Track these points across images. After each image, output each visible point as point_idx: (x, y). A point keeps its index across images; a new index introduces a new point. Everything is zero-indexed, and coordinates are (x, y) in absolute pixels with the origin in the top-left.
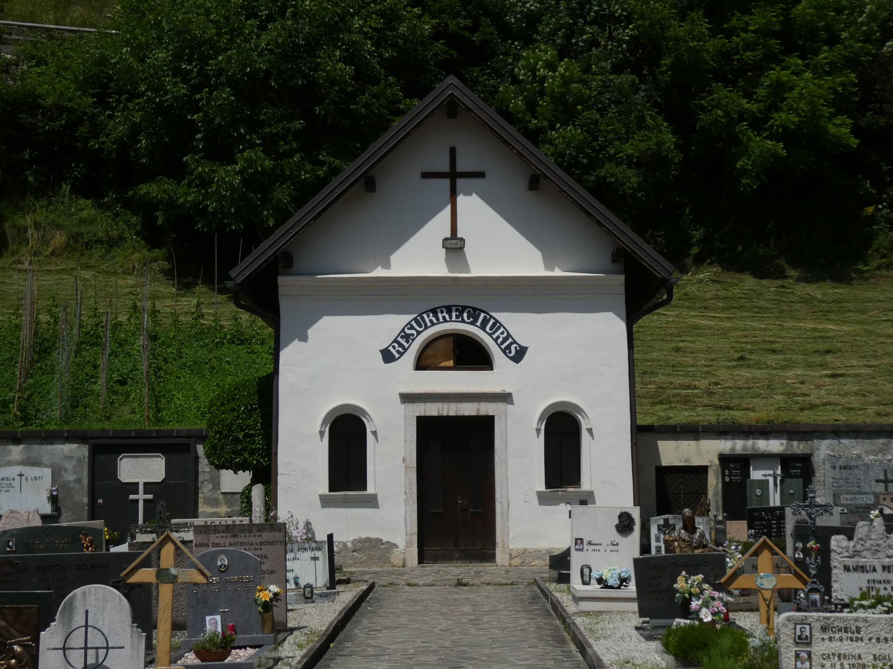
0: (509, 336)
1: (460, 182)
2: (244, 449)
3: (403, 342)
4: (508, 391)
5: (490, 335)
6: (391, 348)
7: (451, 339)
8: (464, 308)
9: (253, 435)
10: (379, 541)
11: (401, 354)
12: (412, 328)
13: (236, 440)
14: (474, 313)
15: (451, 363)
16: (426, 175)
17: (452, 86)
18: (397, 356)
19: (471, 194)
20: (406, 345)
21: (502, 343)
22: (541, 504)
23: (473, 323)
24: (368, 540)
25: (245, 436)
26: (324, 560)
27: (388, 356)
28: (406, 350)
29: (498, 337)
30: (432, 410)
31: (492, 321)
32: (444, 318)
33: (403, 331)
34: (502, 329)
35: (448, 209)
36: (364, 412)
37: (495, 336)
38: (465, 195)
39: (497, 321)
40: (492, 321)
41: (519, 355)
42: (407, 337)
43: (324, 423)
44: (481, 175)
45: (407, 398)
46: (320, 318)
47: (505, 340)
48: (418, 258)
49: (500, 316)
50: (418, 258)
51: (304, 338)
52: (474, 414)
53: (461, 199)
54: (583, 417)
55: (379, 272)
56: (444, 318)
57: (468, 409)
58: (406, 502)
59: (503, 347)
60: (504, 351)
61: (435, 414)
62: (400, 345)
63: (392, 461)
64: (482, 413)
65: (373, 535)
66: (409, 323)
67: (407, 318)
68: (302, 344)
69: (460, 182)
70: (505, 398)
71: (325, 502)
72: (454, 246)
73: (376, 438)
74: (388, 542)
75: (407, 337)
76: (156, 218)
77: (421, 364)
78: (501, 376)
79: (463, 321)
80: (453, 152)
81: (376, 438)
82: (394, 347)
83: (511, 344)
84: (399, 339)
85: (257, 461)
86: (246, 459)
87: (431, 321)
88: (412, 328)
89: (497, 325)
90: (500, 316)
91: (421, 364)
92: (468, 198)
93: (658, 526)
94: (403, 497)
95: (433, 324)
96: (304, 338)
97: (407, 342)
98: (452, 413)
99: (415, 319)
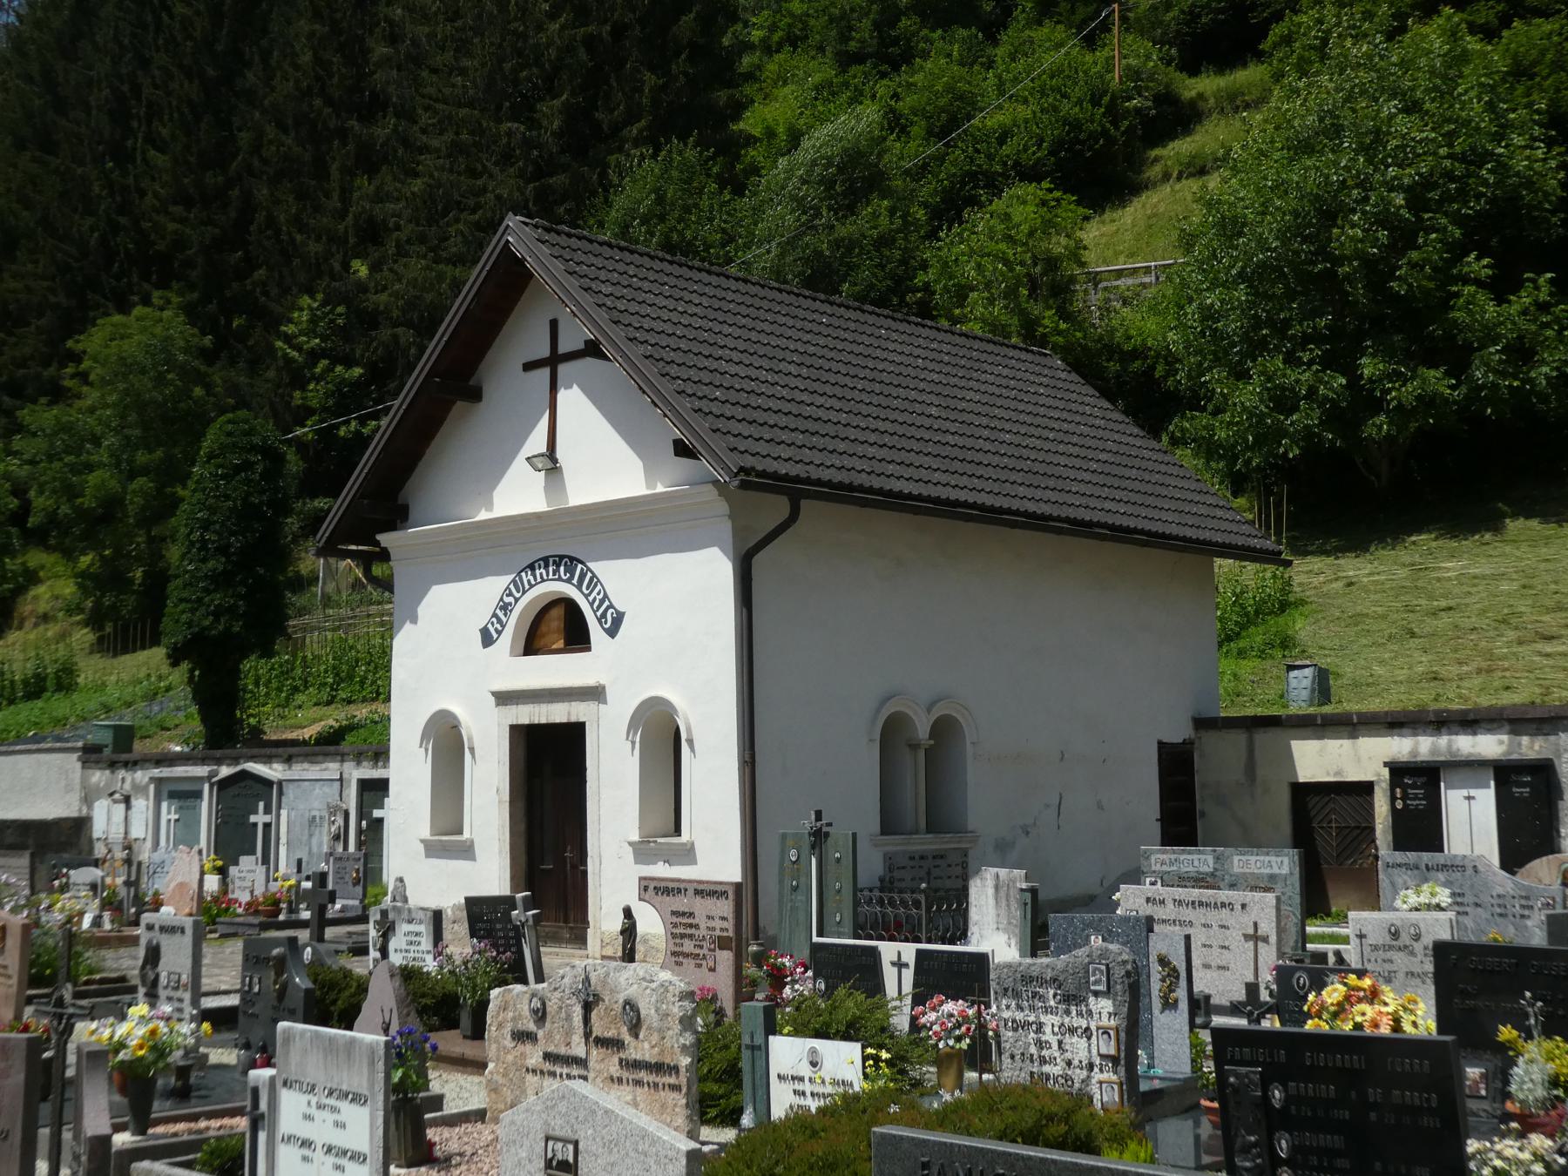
0: (606, 596)
5: (586, 596)
8: (562, 557)
11: (499, 633)
12: (511, 594)
15: (560, 644)
16: (529, 367)
20: (504, 619)
21: (599, 607)
23: (569, 581)
28: (503, 627)
39: (594, 576)
45: (504, 698)
51: (414, 620)
53: (563, 396)
55: (483, 515)
57: (557, 713)
60: (599, 620)
64: (573, 719)
67: (504, 581)
70: (595, 694)
79: (560, 579)
88: (511, 594)
96: (414, 620)
99: (514, 581)
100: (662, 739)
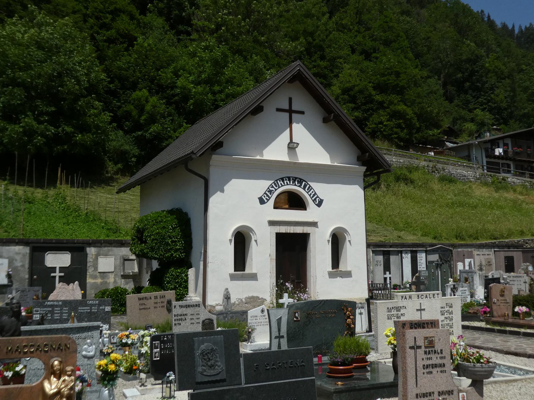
0: (315, 193)
1: (294, 116)
2: (171, 249)
3: (268, 194)
4: (316, 221)
5: (307, 193)
6: (263, 197)
7: (287, 194)
8: (296, 178)
9: (176, 241)
10: (258, 297)
11: (268, 200)
12: (273, 187)
13: (167, 244)
14: (301, 181)
15: (287, 206)
16: (278, 110)
17: (299, 66)
18: (266, 201)
19: (299, 123)
20: (270, 196)
21: (313, 197)
22: (330, 278)
23: (300, 186)
24: (253, 297)
25: (172, 242)
26: (365, 314)
27: (262, 201)
28: (270, 198)
29: (311, 194)
30: (283, 229)
31: (308, 186)
32: (287, 183)
33: (269, 188)
34: (312, 190)
35: (288, 129)
36: (251, 230)
37: (309, 193)
38: (296, 123)
39: (310, 186)
40: (308, 186)
41: (320, 204)
42: (270, 192)
43: (232, 236)
44: (302, 113)
45: (272, 223)
46: (231, 180)
47: (314, 195)
48: (276, 152)
49: (312, 184)
50: (276, 152)
51: (222, 191)
52: (301, 232)
54: (253, 234)
55: (258, 157)
56: (287, 183)
57: (299, 230)
58: (271, 277)
59: (313, 199)
60: (313, 201)
61: (284, 232)
62: (268, 196)
63: (263, 256)
64: (305, 232)
65: (255, 295)
66: (271, 184)
67: (271, 182)
68: (221, 194)
69: (294, 116)
70: (314, 224)
71: (233, 277)
72: (292, 147)
73: (257, 244)
74: (262, 298)
75: (270, 192)
76: (145, 120)
77: (276, 206)
78: (310, 214)
79: (295, 185)
80: (290, 100)
81: (257, 244)
82: (264, 196)
83: (316, 198)
84: (267, 192)
85: (179, 255)
86: (173, 254)
87: (281, 184)
88: (273, 187)
89: (310, 188)
90: (312, 184)
91: (276, 206)
92: (297, 125)
93: (451, 288)
94: (269, 274)
95: (282, 186)
96: (222, 191)
97: (271, 194)
98: (292, 232)
99: (274, 183)
100: (337, 241)
